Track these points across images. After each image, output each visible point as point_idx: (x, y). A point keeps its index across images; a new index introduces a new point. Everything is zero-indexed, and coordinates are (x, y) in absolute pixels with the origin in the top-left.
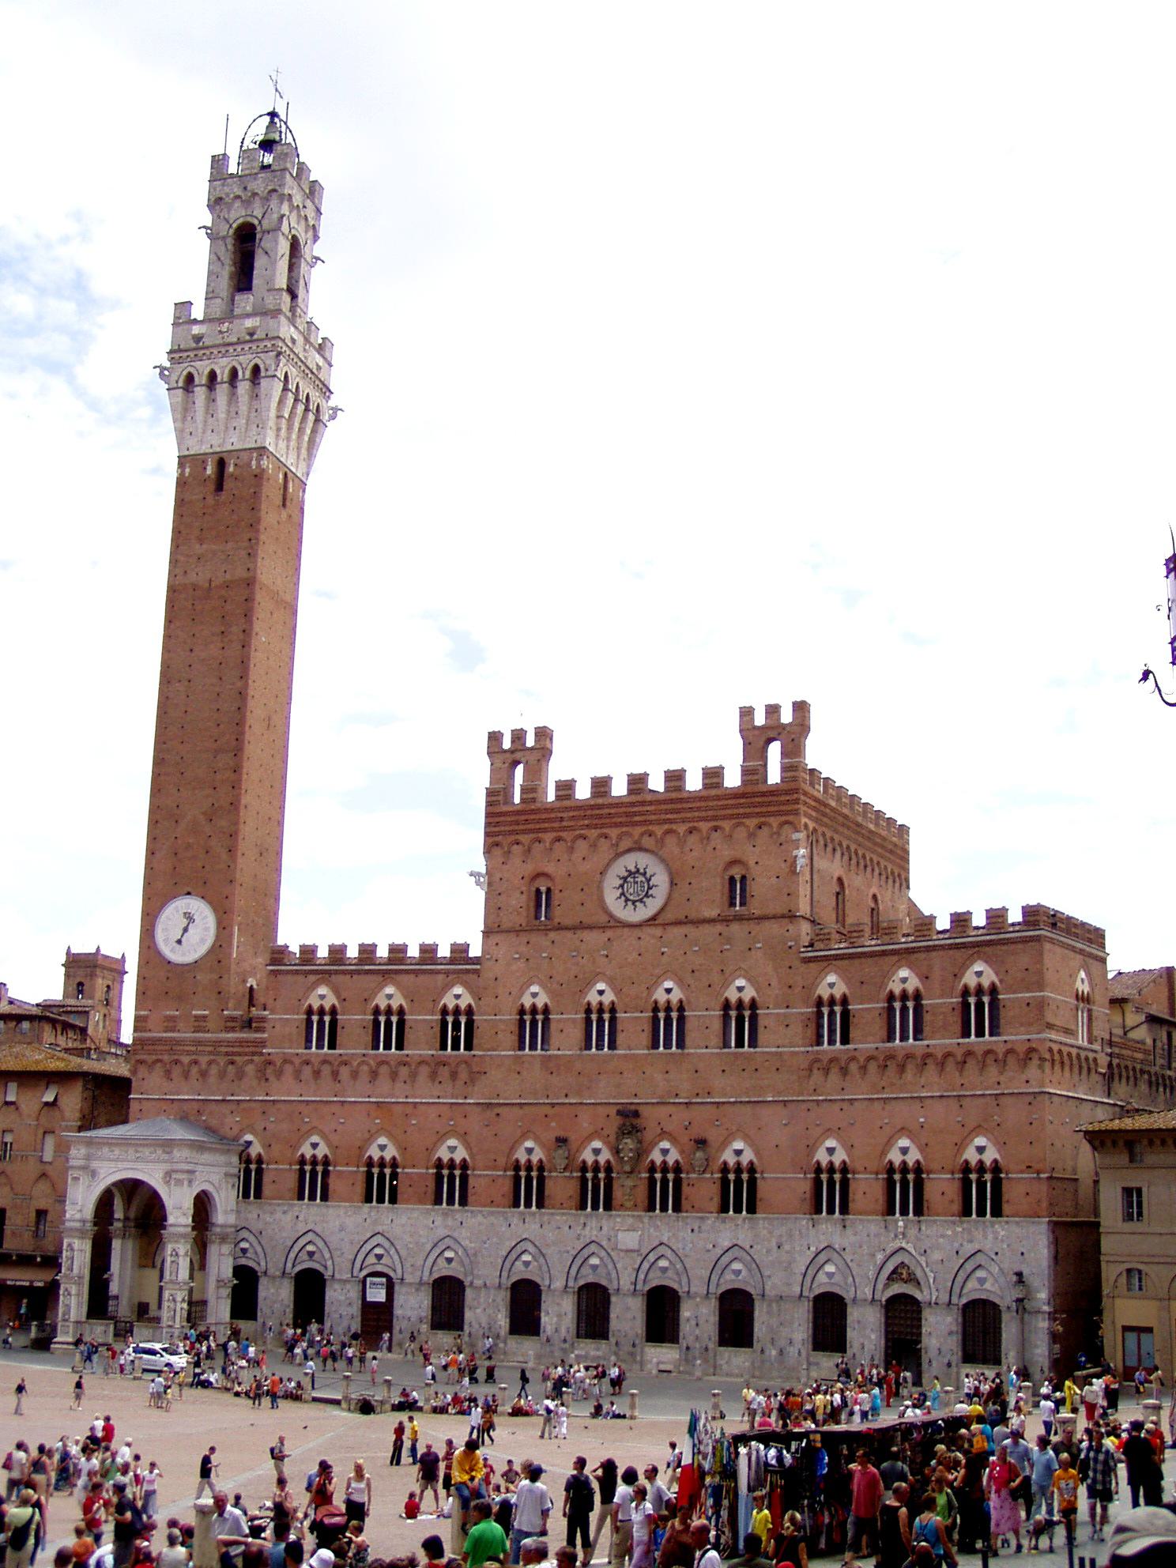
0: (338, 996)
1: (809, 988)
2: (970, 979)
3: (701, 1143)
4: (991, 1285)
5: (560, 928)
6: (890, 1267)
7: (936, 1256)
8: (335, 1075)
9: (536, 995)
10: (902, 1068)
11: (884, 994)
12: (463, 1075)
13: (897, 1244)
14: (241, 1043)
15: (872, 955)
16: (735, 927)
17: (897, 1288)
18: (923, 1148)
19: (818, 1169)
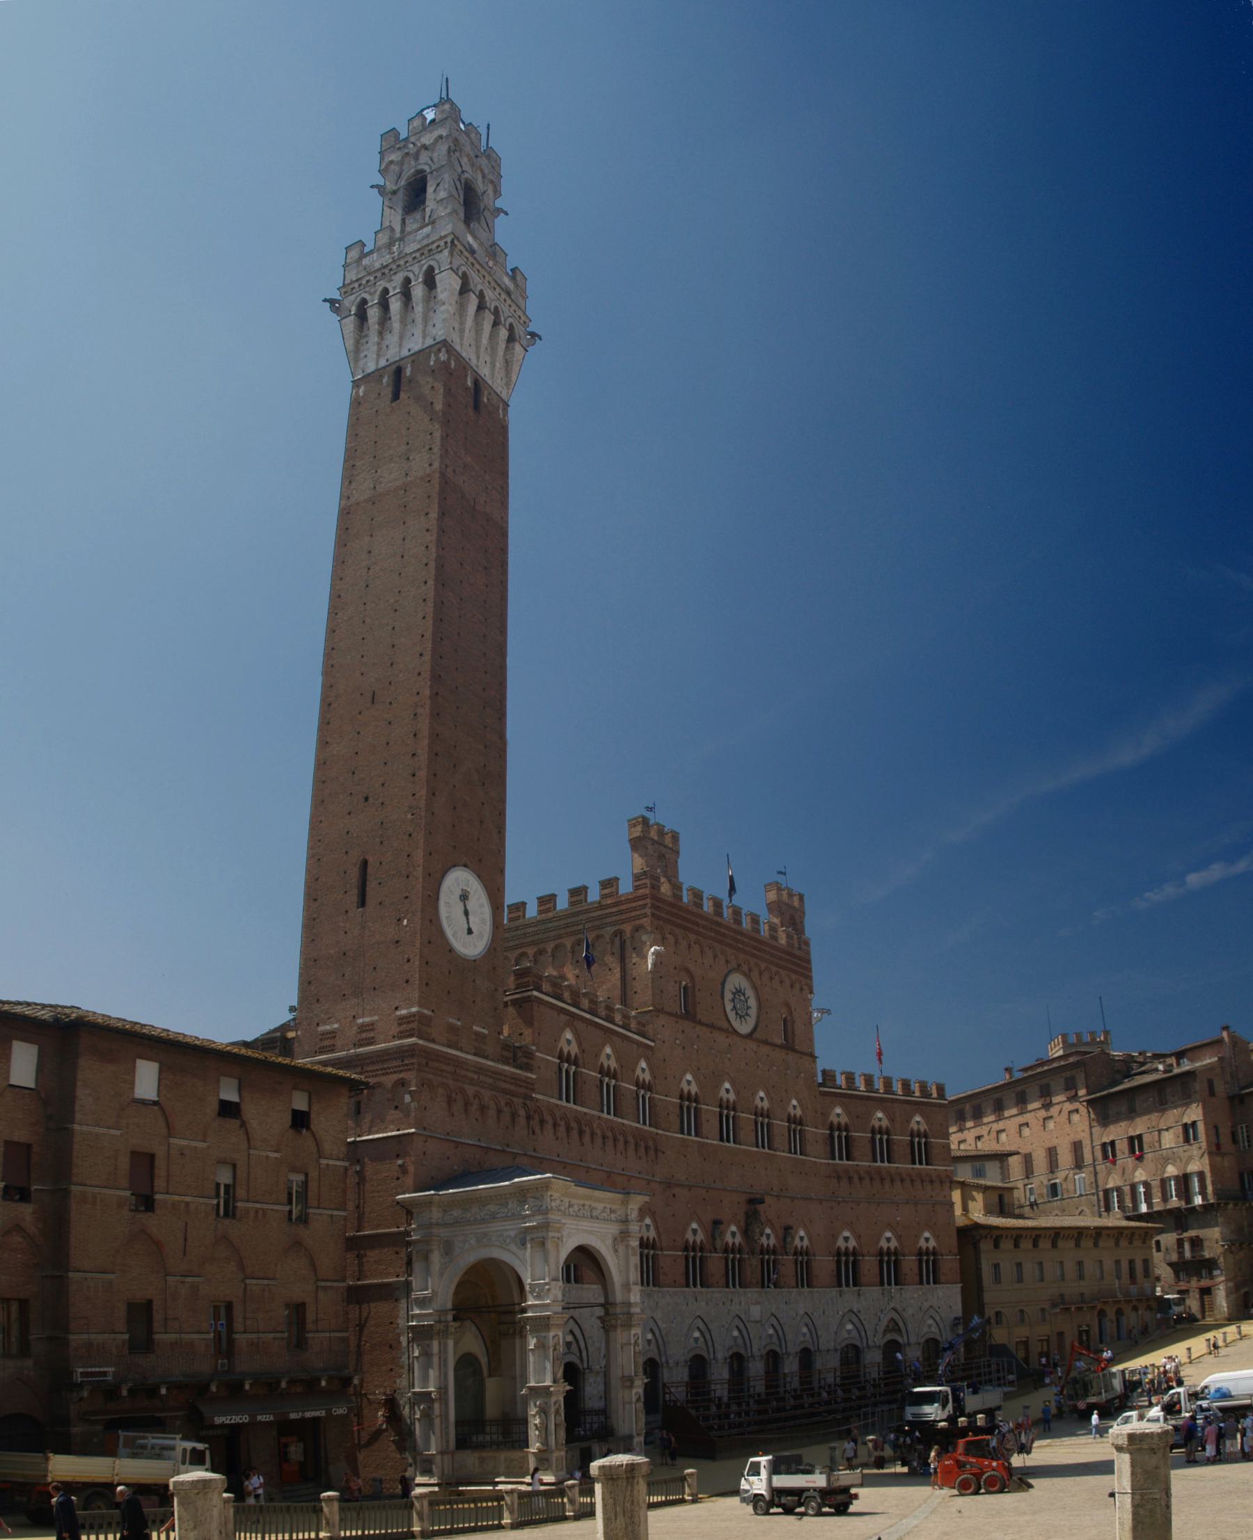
0: (580, 1045)
1: (825, 1115)
2: (913, 1125)
3: (787, 1229)
4: (930, 1328)
5: (700, 1023)
6: (885, 1322)
7: (910, 1311)
8: (581, 1133)
9: (689, 1082)
10: (882, 1179)
11: (869, 1129)
12: (652, 1152)
13: (892, 1305)
14: (515, 1080)
15: (862, 1098)
16: (791, 1057)
17: (889, 1337)
18: (899, 1238)
19: (839, 1254)
